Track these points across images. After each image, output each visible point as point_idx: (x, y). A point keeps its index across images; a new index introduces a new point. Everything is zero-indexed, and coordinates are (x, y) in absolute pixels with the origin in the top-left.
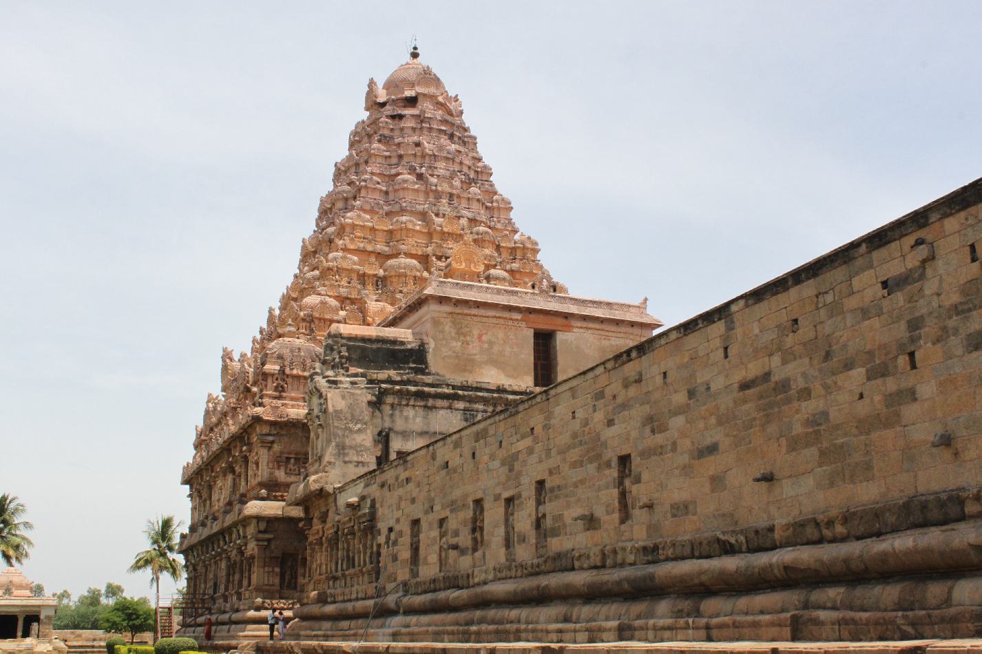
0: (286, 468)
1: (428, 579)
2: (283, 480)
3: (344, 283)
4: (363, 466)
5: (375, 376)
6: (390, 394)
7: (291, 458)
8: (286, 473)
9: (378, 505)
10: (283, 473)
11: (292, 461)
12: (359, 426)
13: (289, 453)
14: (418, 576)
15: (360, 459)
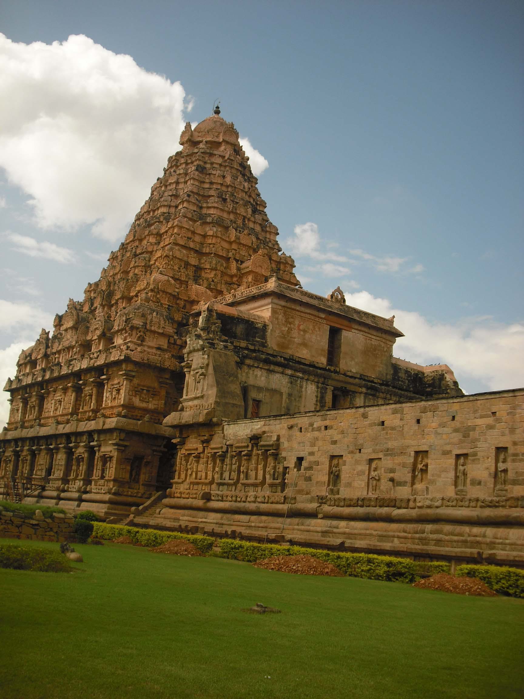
0: (140, 396)
1: (356, 497)
2: (137, 405)
3: (176, 268)
4: (237, 407)
5: (238, 344)
6: (248, 358)
7: (144, 389)
8: (140, 400)
9: (282, 440)
10: (138, 400)
11: (145, 391)
12: (232, 378)
13: (144, 386)
14: (338, 494)
15: (235, 402)
